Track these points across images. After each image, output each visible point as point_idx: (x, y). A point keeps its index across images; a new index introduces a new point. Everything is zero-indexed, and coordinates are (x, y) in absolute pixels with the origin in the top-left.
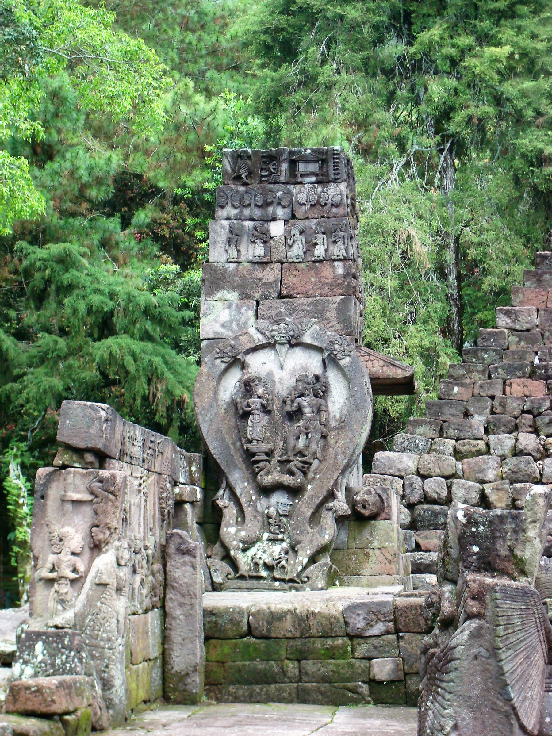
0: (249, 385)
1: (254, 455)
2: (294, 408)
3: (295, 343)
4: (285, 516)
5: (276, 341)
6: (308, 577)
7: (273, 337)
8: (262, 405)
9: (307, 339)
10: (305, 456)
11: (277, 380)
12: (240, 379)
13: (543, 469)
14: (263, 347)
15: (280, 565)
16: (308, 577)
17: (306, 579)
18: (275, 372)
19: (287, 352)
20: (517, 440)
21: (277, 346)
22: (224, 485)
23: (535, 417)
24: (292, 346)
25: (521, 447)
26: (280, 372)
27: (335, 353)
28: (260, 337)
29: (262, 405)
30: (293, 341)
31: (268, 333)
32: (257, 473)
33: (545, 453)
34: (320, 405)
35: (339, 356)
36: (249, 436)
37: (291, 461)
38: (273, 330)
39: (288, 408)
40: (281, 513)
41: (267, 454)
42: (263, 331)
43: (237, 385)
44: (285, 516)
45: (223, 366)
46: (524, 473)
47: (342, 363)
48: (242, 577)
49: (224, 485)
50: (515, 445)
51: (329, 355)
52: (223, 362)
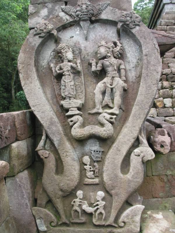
0: (61, 53)
1: (67, 110)
2: (99, 68)
3: (94, 19)
4: (98, 161)
5: (80, 18)
6: (124, 222)
7: (77, 16)
8: (72, 67)
9: (103, 16)
10: (112, 108)
11: (83, 48)
12: (54, 49)
13: (173, 93)
14: (71, 25)
15: (98, 212)
16: (124, 222)
17: (122, 224)
18: (81, 42)
19: (89, 28)
20: (162, 84)
21: (82, 23)
22: (44, 137)
23: (167, 76)
24: (92, 22)
25: (164, 86)
26: (85, 42)
27: (128, 23)
28: (68, 17)
29: (72, 67)
30: (93, 18)
31: (73, 14)
32: (72, 126)
33: (172, 88)
34: (120, 64)
35: (131, 25)
36: (63, 95)
37: (100, 113)
38: (77, 11)
39: (94, 68)
40: (95, 160)
41: (79, 109)
42: (70, 13)
43: (52, 54)
44: (98, 161)
45: (40, 40)
46: (167, 95)
47: (134, 31)
48: (64, 224)
49: (44, 137)
50: (162, 85)
51: (122, 26)
52: (40, 37)
